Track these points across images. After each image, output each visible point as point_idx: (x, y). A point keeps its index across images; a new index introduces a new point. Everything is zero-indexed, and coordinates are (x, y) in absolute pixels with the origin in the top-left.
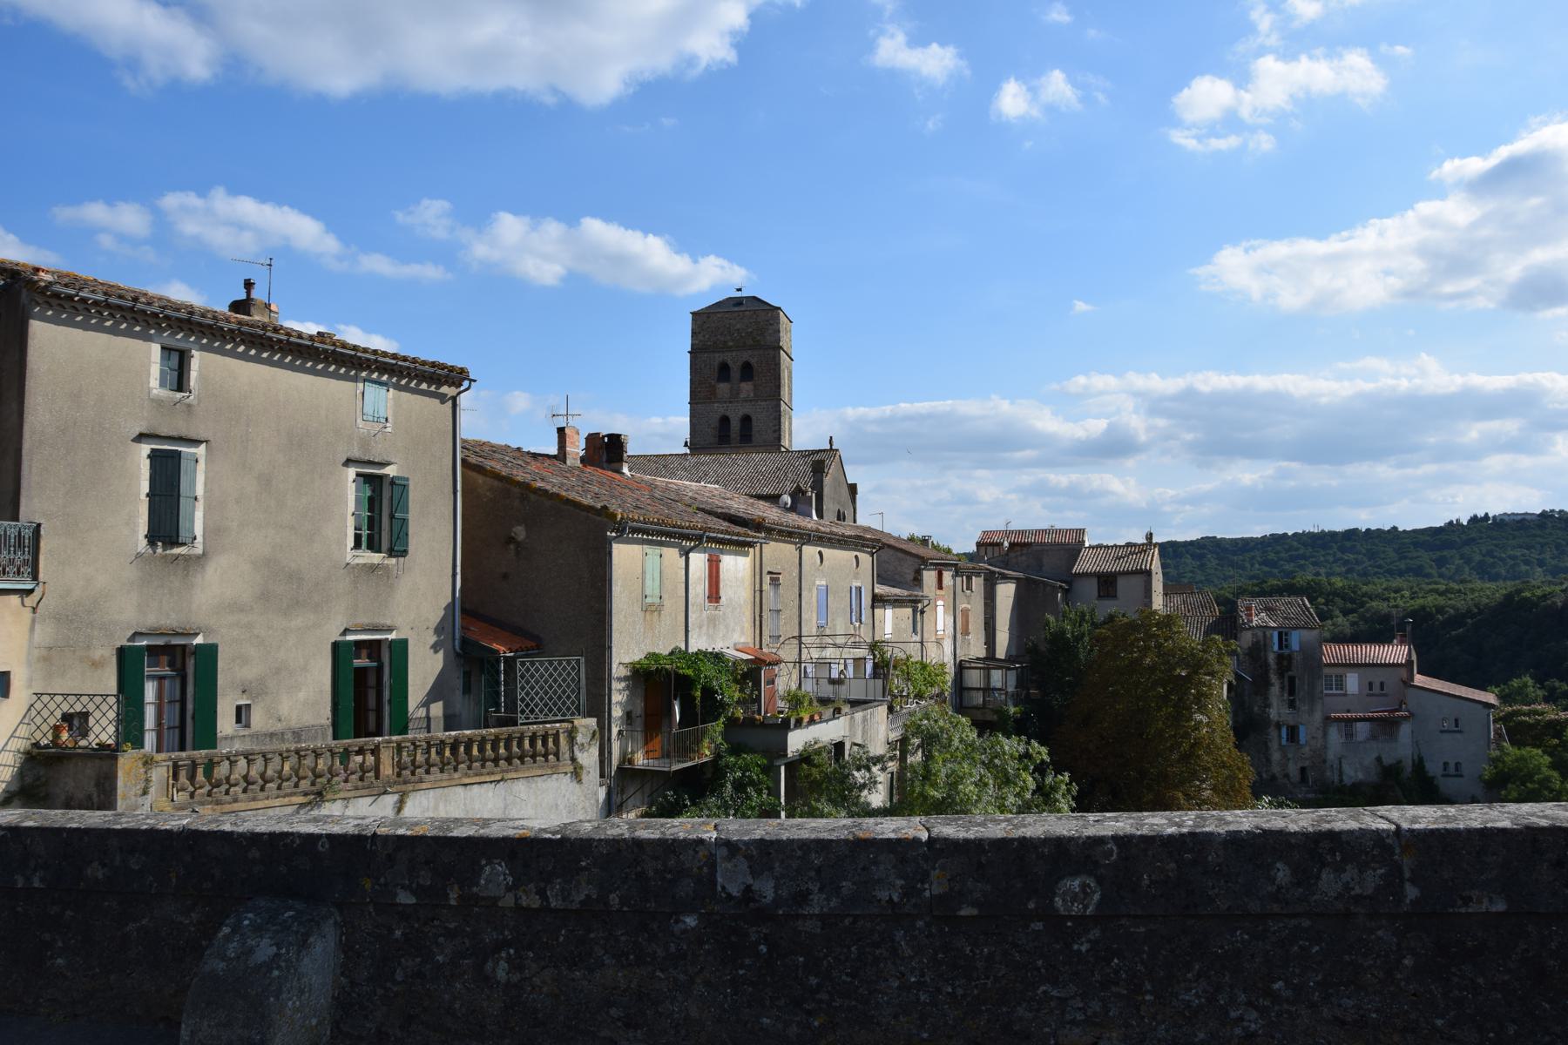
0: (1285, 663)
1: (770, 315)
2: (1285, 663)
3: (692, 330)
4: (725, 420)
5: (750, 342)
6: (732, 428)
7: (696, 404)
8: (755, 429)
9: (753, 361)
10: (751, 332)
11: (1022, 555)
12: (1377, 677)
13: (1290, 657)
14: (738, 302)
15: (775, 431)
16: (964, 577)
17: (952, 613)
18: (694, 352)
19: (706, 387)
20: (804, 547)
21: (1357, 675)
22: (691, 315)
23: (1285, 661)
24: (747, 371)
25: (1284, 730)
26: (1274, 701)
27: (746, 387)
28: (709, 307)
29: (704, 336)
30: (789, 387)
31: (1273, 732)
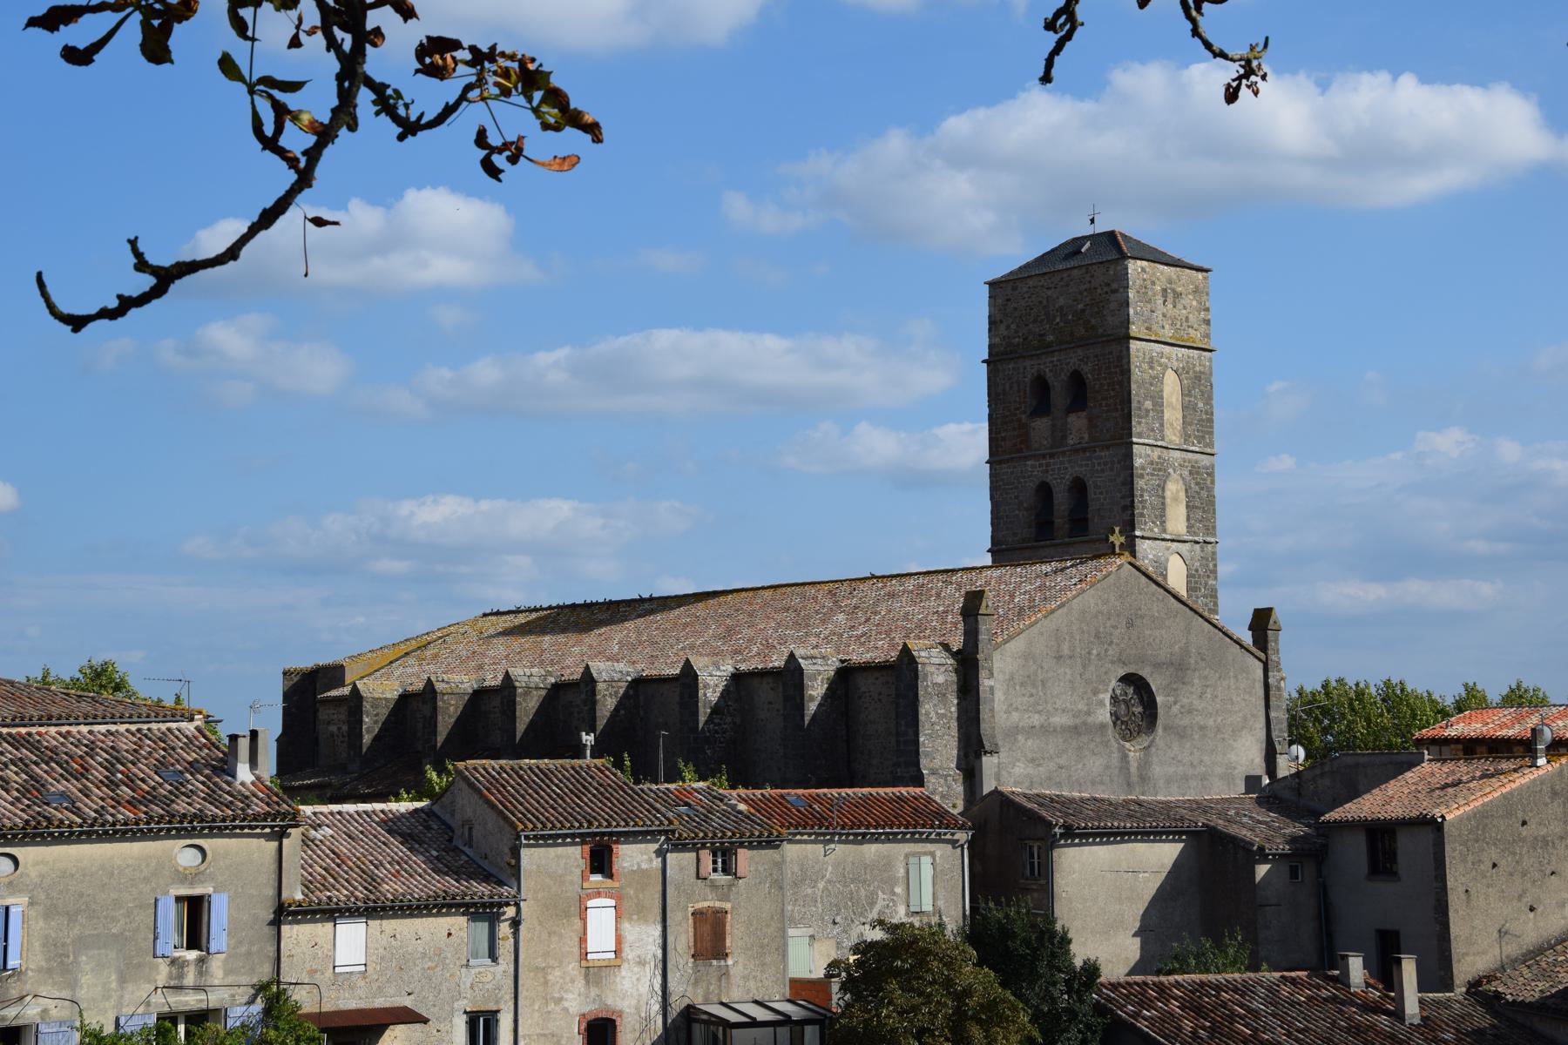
3: (990, 317)
4: (1045, 491)
6: (1055, 508)
7: (1000, 462)
8: (1093, 506)
9: (1086, 369)
10: (1083, 311)
11: (1322, 775)
14: (1072, 249)
15: (1125, 508)
16: (707, 857)
17: (659, 918)
18: (994, 362)
19: (1014, 429)
27: (1077, 422)
28: (1027, 266)
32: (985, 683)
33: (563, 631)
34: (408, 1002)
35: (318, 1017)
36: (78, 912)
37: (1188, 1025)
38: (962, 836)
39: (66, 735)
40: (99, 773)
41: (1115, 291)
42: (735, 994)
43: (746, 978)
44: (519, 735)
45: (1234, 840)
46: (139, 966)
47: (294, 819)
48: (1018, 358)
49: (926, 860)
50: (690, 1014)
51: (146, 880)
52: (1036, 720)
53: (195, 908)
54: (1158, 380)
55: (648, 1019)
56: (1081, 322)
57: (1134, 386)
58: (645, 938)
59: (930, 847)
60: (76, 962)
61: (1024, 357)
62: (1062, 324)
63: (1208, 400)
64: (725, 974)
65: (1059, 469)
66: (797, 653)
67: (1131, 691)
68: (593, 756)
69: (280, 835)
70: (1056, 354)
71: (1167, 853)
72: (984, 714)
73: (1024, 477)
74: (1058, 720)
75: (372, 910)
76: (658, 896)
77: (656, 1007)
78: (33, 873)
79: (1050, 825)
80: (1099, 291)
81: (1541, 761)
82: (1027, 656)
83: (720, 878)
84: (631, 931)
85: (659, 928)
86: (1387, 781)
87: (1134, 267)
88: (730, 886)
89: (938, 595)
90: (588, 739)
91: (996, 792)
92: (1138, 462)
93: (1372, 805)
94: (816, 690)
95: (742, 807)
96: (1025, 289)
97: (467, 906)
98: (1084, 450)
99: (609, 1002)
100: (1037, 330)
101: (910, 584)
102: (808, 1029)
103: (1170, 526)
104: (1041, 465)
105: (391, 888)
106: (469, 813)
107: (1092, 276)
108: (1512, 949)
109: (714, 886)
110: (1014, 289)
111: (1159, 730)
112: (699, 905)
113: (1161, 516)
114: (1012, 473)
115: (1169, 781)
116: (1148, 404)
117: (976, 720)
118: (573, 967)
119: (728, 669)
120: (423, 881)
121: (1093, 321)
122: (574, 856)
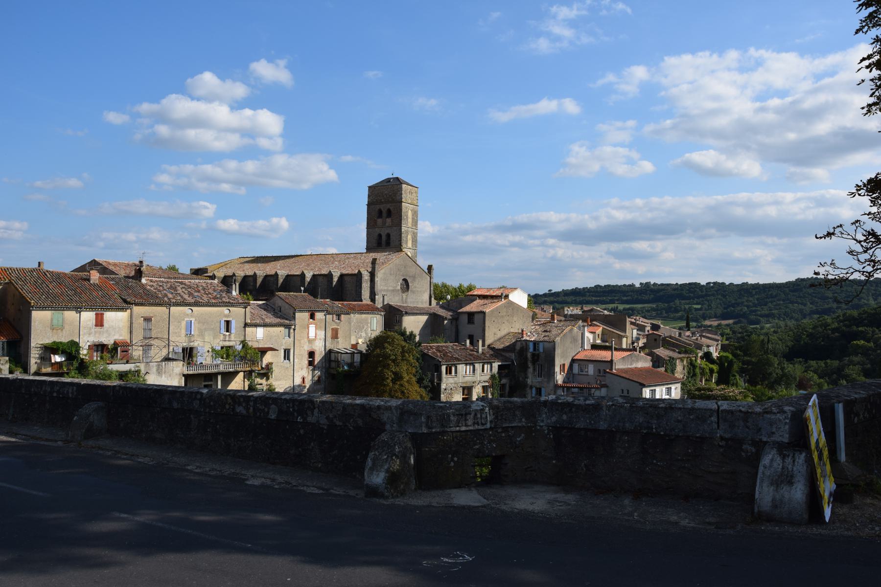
0: (536, 358)
2: (536, 358)
4: (380, 236)
5: (391, 200)
8: (391, 240)
9: (391, 208)
11: (454, 302)
12: (602, 367)
13: (538, 355)
14: (388, 180)
15: (399, 241)
16: (335, 316)
18: (369, 205)
20: (171, 308)
21: (593, 365)
23: (536, 357)
24: (389, 213)
25: (534, 389)
26: (530, 375)
27: (389, 220)
28: (377, 183)
30: (413, 219)
31: (528, 390)
32: (376, 279)
33: (263, 263)
34: (272, 346)
35: (258, 348)
36: (205, 323)
37: (439, 354)
38: (383, 313)
39: (190, 282)
40: (202, 291)
41: (399, 191)
42: (340, 347)
43: (342, 343)
44: (257, 287)
45: (440, 316)
46: (217, 335)
47: (249, 304)
49: (375, 319)
50: (330, 351)
51: (218, 316)
52: (386, 288)
53: (228, 323)
54: (407, 212)
55: (321, 352)
57: (403, 213)
58: (321, 334)
59: (376, 315)
60: (204, 334)
63: (417, 218)
64: (338, 342)
66: (332, 271)
67: (404, 282)
68: (303, 292)
69: (245, 308)
71: (425, 318)
72: (376, 287)
74: (390, 288)
75: (265, 325)
76: (324, 325)
77: (323, 349)
78: (196, 313)
79: (402, 312)
81: (503, 300)
82: (384, 274)
83: (337, 321)
84: (319, 332)
85: (324, 332)
86: (470, 303)
87: (404, 186)
88: (340, 323)
89: (360, 258)
90: (302, 289)
91: (388, 304)
92: (403, 230)
93: (468, 308)
94: (335, 279)
95: (340, 305)
97: (284, 325)
99: (314, 348)
101: (352, 256)
102: (355, 355)
103: (408, 245)
105: (268, 321)
106: (280, 305)
108: (496, 339)
109: (336, 323)
110: (375, 188)
111: (410, 291)
112: (333, 327)
113: (407, 243)
115: (411, 303)
116: (405, 217)
117: (374, 288)
118: (306, 340)
119: (312, 274)
120: (270, 319)
122: (307, 315)
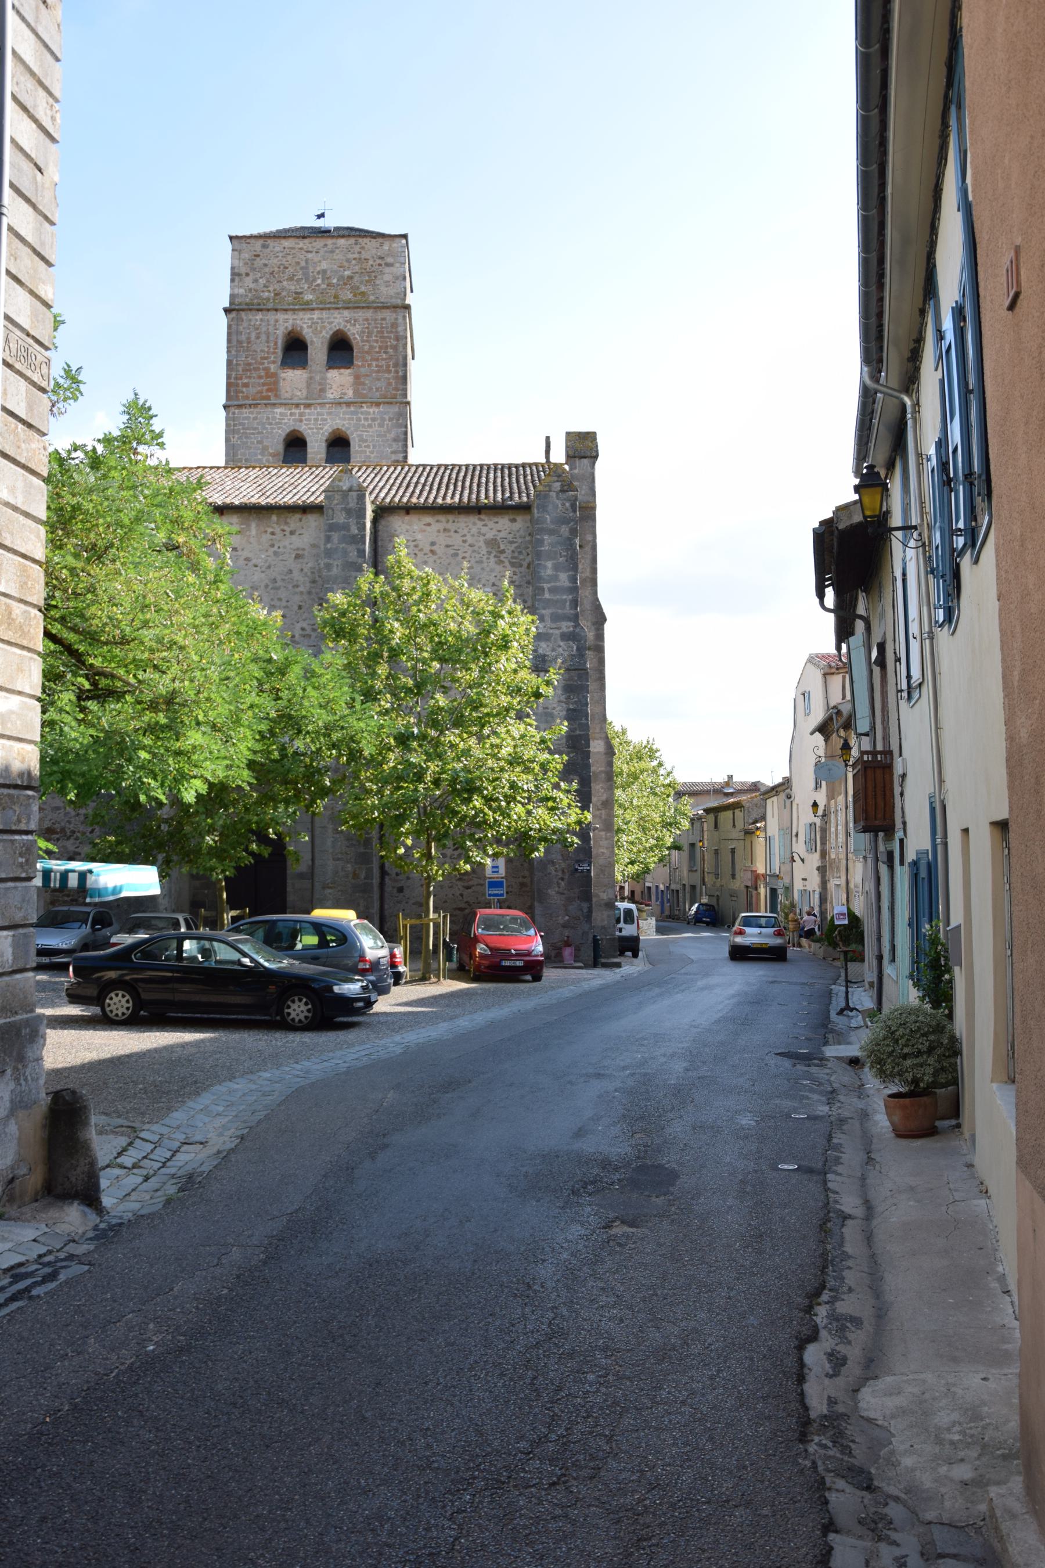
1: (386, 247)
3: (233, 268)
9: (354, 333)
10: (350, 278)
19: (260, 377)
22: (228, 246)
27: (340, 380)
29: (256, 281)
48: (268, 310)
56: (348, 286)
61: (276, 310)
62: (324, 286)
65: (316, 420)
70: (316, 312)
73: (271, 424)
80: (371, 262)
96: (277, 249)
98: (348, 404)
100: (293, 288)
104: (291, 414)
107: (363, 248)
110: (264, 246)
114: (255, 418)
121: (363, 289)
